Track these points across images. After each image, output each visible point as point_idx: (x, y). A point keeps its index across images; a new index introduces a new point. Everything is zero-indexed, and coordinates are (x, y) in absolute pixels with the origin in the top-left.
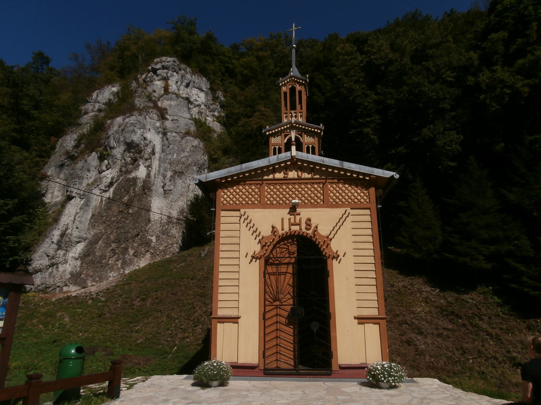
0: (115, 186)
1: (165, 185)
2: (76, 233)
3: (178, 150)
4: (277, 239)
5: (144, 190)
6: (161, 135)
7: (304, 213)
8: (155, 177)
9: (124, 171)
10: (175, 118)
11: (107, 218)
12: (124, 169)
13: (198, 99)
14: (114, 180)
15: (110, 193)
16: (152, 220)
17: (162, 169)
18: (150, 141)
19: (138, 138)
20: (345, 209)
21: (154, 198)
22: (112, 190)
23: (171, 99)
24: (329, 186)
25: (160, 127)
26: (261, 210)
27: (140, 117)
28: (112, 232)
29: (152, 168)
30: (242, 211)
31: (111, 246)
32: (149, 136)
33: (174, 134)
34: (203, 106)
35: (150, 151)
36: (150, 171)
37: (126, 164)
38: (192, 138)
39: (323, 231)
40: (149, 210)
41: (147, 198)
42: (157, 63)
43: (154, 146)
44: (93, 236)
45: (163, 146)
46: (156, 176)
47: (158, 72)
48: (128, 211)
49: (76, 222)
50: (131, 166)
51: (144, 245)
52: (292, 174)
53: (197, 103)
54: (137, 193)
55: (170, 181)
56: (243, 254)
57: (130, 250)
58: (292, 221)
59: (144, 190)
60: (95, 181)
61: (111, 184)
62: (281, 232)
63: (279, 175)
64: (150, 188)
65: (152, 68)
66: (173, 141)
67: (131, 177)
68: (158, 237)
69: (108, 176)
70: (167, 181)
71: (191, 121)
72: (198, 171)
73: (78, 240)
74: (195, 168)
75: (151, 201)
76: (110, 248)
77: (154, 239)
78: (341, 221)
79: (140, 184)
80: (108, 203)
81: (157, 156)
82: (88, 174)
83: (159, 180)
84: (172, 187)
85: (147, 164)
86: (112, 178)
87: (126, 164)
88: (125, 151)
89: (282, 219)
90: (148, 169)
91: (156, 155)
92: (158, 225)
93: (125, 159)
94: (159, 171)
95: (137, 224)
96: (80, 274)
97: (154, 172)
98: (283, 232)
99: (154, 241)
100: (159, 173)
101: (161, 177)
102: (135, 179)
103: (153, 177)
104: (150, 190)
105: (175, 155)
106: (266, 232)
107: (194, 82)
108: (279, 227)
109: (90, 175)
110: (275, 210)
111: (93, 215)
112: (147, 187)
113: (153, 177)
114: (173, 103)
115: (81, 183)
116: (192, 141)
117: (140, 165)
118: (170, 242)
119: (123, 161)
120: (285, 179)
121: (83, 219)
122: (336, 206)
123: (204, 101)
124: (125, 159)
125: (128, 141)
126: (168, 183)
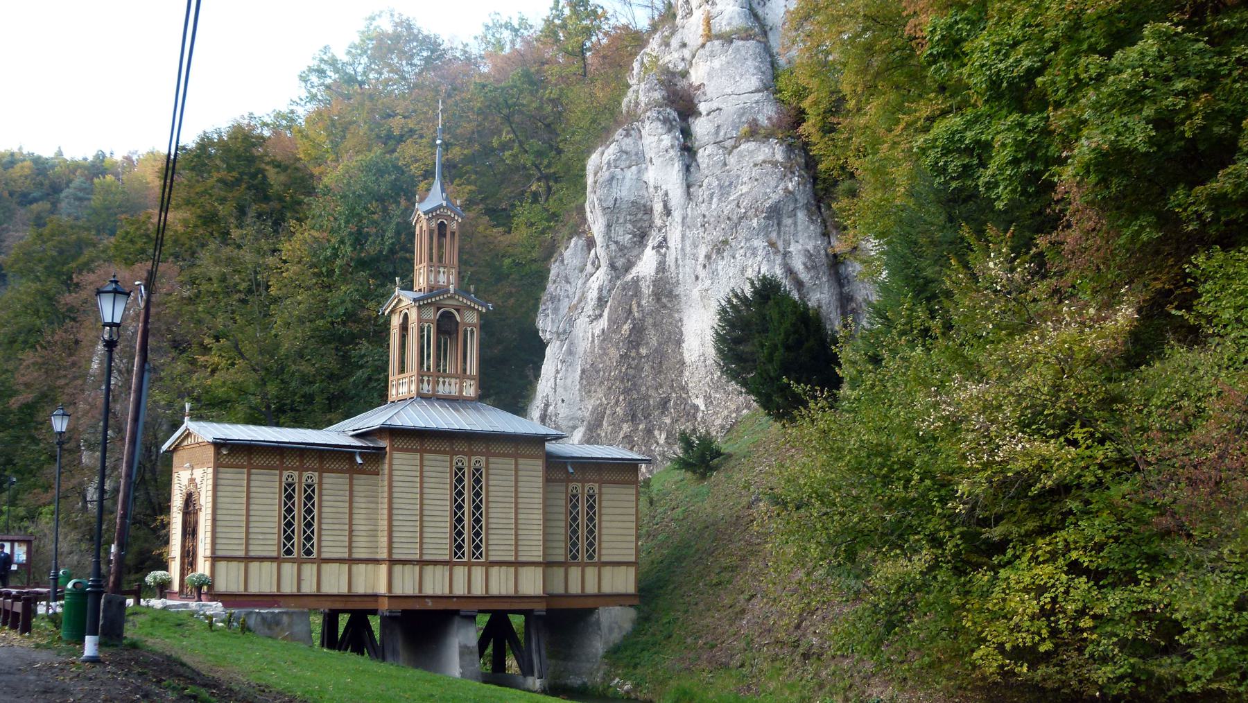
1: (697, 278)
2: (563, 411)
3: (721, 187)
5: (658, 300)
6: (677, 165)
8: (677, 266)
9: (619, 269)
10: (714, 105)
12: (620, 263)
14: (605, 293)
15: (603, 323)
16: (687, 359)
17: (688, 243)
19: (630, 189)
22: (606, 314)
23: (712, 55)
25: (672, 146)
27: (627, 140)
28: (617, 401)
29: (668, 248)
31: (621, 429)
32: (651, 175)
36: (665, 256)
37: (621, 250)
38: (752, 145)
40: (679, 343)
41: (671, 316)
43: (666, 194)
44: (592, 413)
45: (688, 186)
46: (680, 262)
48: (638, 353)
50: (635, 252)
55: (705, 266)
57: (656, 432)
59: (658, 300)
60: (580, 301)
61: (601, 302)
64: (671, 292)
67: (629, 277)
68: (708, 398)
70: (699, 268)
71: (757, 96)
72: (767, 226)
73: (571, 424)
74: (755, 222)
75: (681, 320)
76: (621, 435)
77: (700, 403)
79: (646, 289)
80: (604, 340)
81: (677, 215)
83: (687, 269)
84: (708, 283)
85: (656, 243)
86: (600, 289)
87: (621, 250)
90: (658, 252)
92: (703, 371)
93: (617, 243)
94: (683, 249)
95: (662, 377)
97: (673, 256)
99: (702, 407)
100: (685, 255)
101: (689, 262)
102: (636, 281)
103: (673, 268)
104: (672, 296)
105: (715, 200)
109: (571, 291)
111: (583, 371)
112: (665, 291)
113: (673, 268)
114: (717, 63)
115: (556, 310)
116: (752, 152)
117: (646, 246)
118: (733, 407)
119: (613, 247)
121: (569, 381)
124: (617, 243)
125: (605, 205)
126: (702, 273)
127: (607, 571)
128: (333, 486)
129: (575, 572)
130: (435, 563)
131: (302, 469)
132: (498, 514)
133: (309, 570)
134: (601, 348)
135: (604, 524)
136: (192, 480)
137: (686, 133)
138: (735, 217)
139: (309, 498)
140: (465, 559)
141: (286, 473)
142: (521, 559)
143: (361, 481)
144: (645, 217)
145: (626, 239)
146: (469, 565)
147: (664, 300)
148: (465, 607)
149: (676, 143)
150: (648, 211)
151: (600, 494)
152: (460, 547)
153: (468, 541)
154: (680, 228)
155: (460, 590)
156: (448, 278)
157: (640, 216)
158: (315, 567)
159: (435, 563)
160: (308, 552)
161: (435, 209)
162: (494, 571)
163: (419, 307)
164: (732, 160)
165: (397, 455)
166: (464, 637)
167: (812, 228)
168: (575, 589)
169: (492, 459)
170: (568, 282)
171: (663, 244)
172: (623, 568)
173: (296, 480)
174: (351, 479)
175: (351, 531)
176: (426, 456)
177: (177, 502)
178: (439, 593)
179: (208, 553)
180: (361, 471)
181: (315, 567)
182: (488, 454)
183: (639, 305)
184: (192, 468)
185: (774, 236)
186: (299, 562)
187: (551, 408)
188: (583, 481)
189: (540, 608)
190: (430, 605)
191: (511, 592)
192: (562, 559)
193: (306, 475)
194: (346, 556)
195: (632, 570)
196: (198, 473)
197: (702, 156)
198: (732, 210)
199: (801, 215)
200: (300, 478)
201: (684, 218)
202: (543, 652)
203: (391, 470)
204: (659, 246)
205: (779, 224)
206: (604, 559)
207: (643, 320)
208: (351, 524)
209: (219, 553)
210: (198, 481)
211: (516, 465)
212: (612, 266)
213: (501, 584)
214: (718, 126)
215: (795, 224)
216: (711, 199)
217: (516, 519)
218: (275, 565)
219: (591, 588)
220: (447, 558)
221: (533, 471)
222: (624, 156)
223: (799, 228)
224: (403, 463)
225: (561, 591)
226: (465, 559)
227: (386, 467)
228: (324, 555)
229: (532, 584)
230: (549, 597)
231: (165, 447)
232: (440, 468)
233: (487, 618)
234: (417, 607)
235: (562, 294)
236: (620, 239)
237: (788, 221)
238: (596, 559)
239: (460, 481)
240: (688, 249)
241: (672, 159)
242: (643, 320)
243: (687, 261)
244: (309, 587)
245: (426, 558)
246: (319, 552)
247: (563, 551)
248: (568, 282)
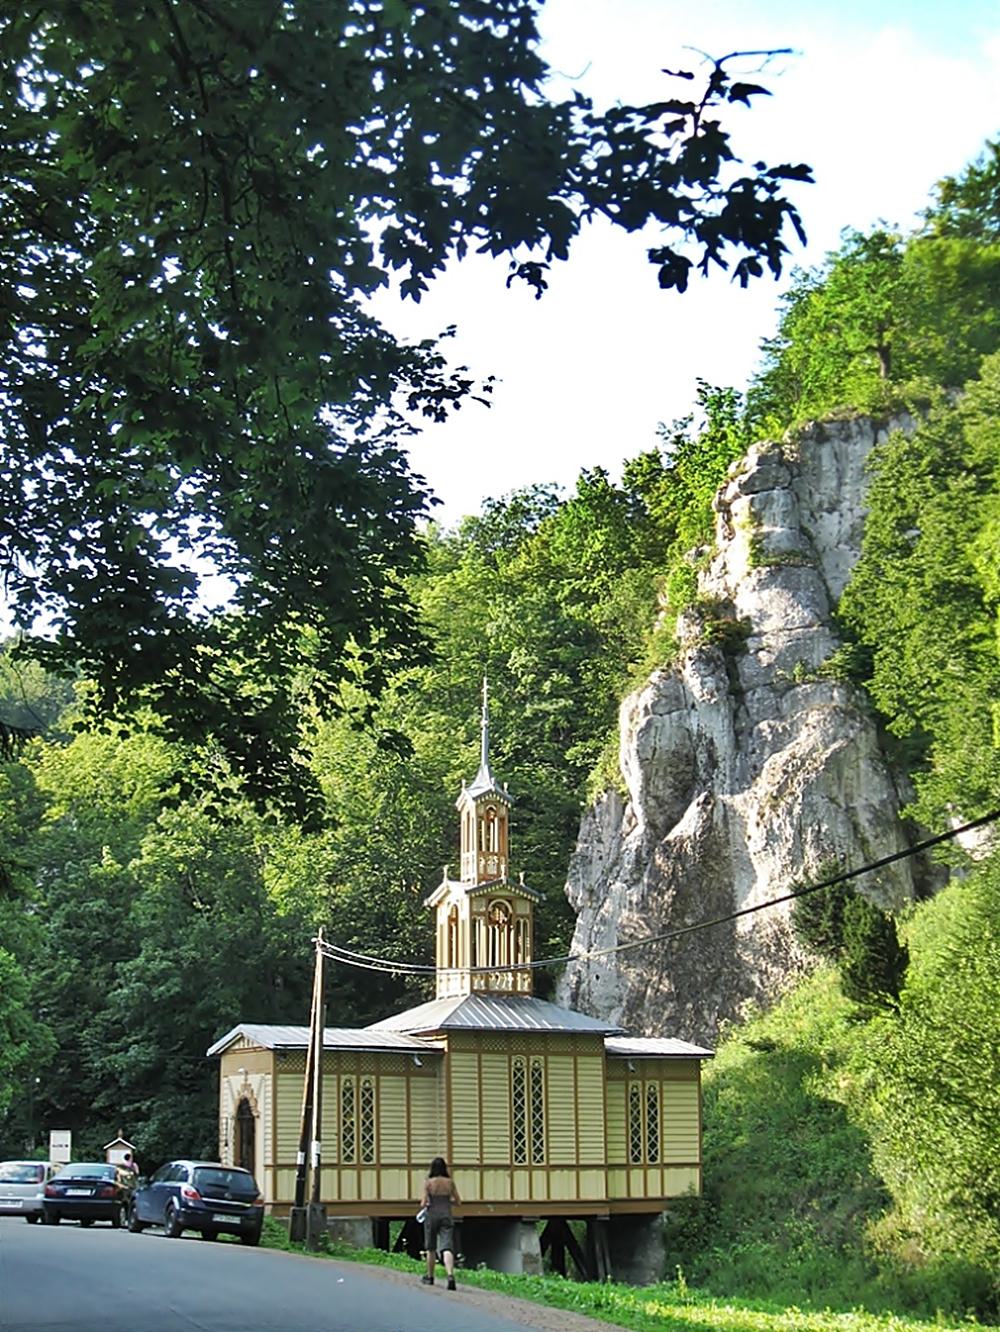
14: (644, 855)
18: (700, 736)
21: (738, 877)
32: (693, 723)
43: (711, 742)
45: (737, 733)
47: (734, 508)
54: (692, 875)
57: (706, 1013)
59: (705, 862)
60: (615, 864)
64: (718, 853)
66: (757, 713)
75: (731, 885)
82: (601, 847)
87: (660, 806)
91: (721, 765)
93: (655, 798)
95: (711, 949)
104: (717, 856)
106: (237, 1097)
113: (721, 825)
114: (766, 594)
117: (690, 802)
119: (652, 802)
125: (643, 756)
127: (669, 1173)
128: (391, 1089)
129: (637, 1175)
130: (497, 1167)
131: (359, 1073)
132: (558, 1115)
133: (369, 1176)
135: (665, 1124)
136: (246, 1086)
137: (733, 673)
139: (368, 1102)
140: (526, 1163)
141: (344, 1077)
142: (582, 1162)
143: (417, 1082)
144: (689, 769)
145: (666, 793)
146: (530, 1169)
148: (526, 1212)
149: (721, 684)
150: (691, 761)
151: (661, 1092)
152: (520, 1151)
153: (529, 1142)
155: (522, 1195)
156: (498, 867)
157: (682, 767)
158: (374, 1173)
159: (497, 1167)
160: (368, 1158)
161: (484, 795)
162: (555, 1175)
163: (471, 899)
165: (454, 1056)
166: (530, 1243)
167: (877, 779)
168: (637, 1193)
169: (550, 1058)
170: (600, 841)
172: (687, 1169)
173: (354, 1083)
174: (408, 1082)
175: (409, 1135)
176: (484, 1057)
177: (228, 1109)
178: (501, 1199)
179: (269, 1162)
180: (419, 1073)
181: (374, 1173)
182: (546, 1054)
184: (247, 1073)
185: (835, 789)
186: (359, 1168)
187: (584, 985)
188: (643, 1079)
189: (603, 1212)
190: (492, 1211)
191: (573, 1197)
192: (624, 1161)
193: (363, 1078)
194: (405, 1161)
195: (696, 1172)
196: (254, 1080)
198: (788, 761)
199: (863, 765)
200: (358, 1080)
202: (608, 1261)
203: (449, 1072)
204: (706, 802)
205: (839, 778)
206: (666, 1160)
208: (409, 1128)
209: (280, 1161)
210: (254, 1087)
211: (575, 1063)
212: (651, 824)
213: (563, 1188)
215: (858, 776)
217: (577, 1120)
218: (335, 1172)
219: (654, 1192)
220: (508, 1162)
221: (592, 1069)
222: (664, 701)
223: (863, 780)
224: (462, 1065)
225: (623, 1195)
226: (526, 1163)
227: (444, 1068)
228: (383, 1161)
229: (593, 1187)
230: (610, 1202)
231: (211, 1051)
232: (498, 1068)
233: (545, 1222)
234: (480, 1213)
235: (596, 855)
236: (660, 793)
237: (847, 772)
238: (658, 1161)
239: (519, 1081)
244: (369, 1194)
245: (485, 1162)
246: (378, 1158)
247: (624, 1153)
248: (600, 841)
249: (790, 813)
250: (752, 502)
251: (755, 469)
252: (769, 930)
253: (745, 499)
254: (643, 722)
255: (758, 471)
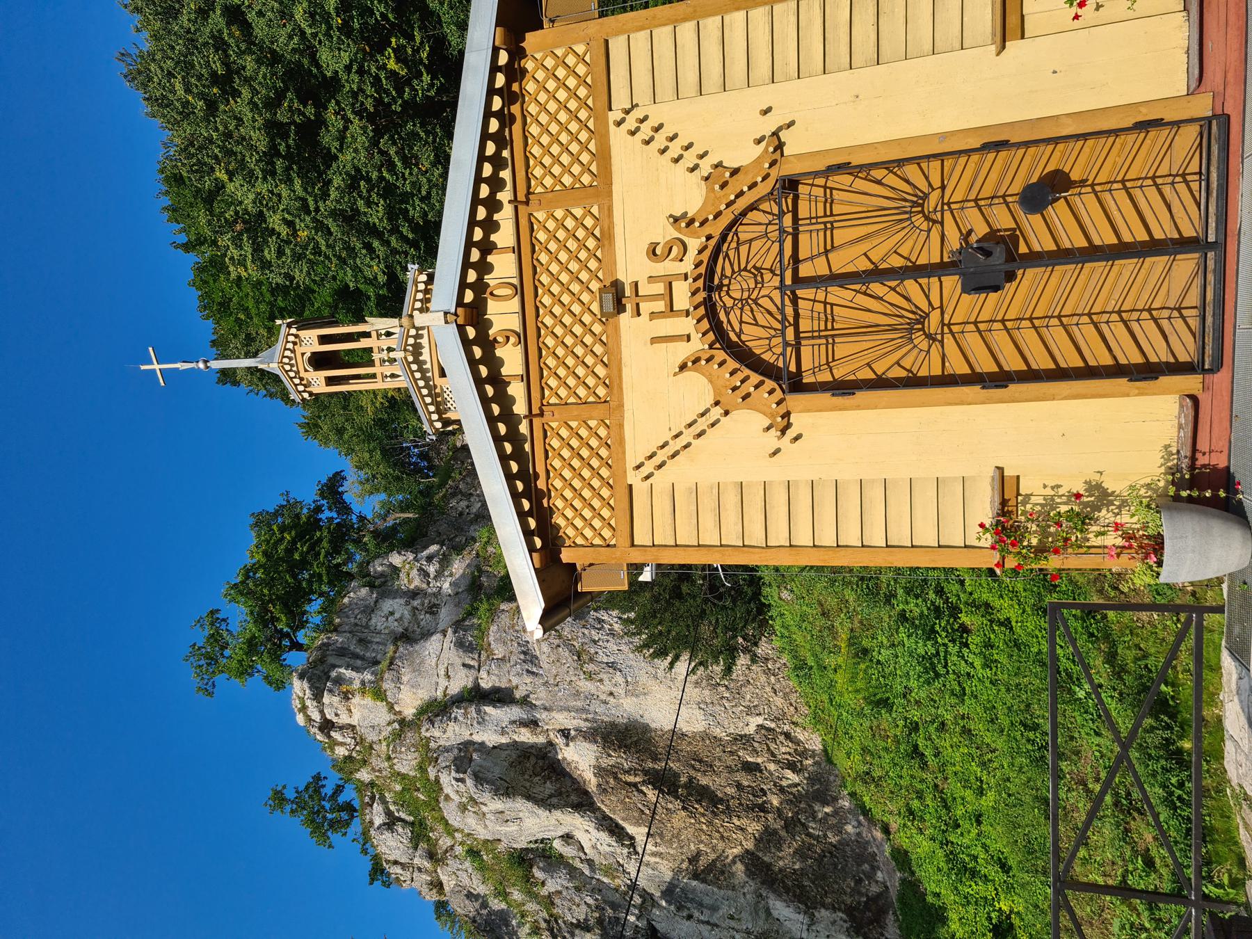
0: (621, 822)
4: (720, 355)
6: (488, 709)
7: (631, 266)
10: (442, 672)
11: (702, 842)
13: (397, 615)
20: (612, 127)
22: (631, 829)
24: (539, 190)
25: (466, 709)
26: (628, 415)
30: (633, 478)
33: (483, 674)
34: (416, 603)
35: (529, 735)
38: (493, 628)
39: (691, 196)
42: (309, 719)
43: (514, 722)
46: (590, 716)
48: (685, 786)
49: (714, 920)
51: (773, 746)
52: (503, 315)
53: (407, 615)
55: (601, 681)
56: (776, 472)
58: (660, 306)
61: (616, 831)
62: (698, 345)
63: (511, 359)
65: (321, 729)
68: (749, 711)
69: (594, 840)
73: (763, 916)
78: (654, 136)
84: (619, 678)
87: (560, 794)
88: (529, 798)
89: (655, 340)
90: (573, 739)
96: (850, 911)
98: (696, 337)
99: (760, 720)
100: (583, 710)
102: (600, 771)
106: (697, 391)
107: (356, 625)
108: (683, 351)
110: (625, 372)
114: (405, 679)
118: (763, 678)
119: (554, 800)
120: (523, 338)
122: (603, 157)
123: (402, 601)
124: (551, 796)
126: (608, 687)
134: (670, 842)
138: (557, 642)
144: (533, 760)
145: (549, 787)
147: (629, 742)
154: (554, 714)
164: (499, 652)
171: (565, 733)
183: (628, 772)
197: (486, 684)
201: (545, 709)
207: (646, 772)
214: (464, 665)
216: (533, 673)
236: (548, 792)
240: (579, 704)
241: (478, 712)
242: (646, 772)
243: (592, 708)
249: (595, 642)
250: (330, 691)
251: (306, 685)
252: (707, 692)
253: (326, 699)
254: (470, 782)
255: (309, 681)
